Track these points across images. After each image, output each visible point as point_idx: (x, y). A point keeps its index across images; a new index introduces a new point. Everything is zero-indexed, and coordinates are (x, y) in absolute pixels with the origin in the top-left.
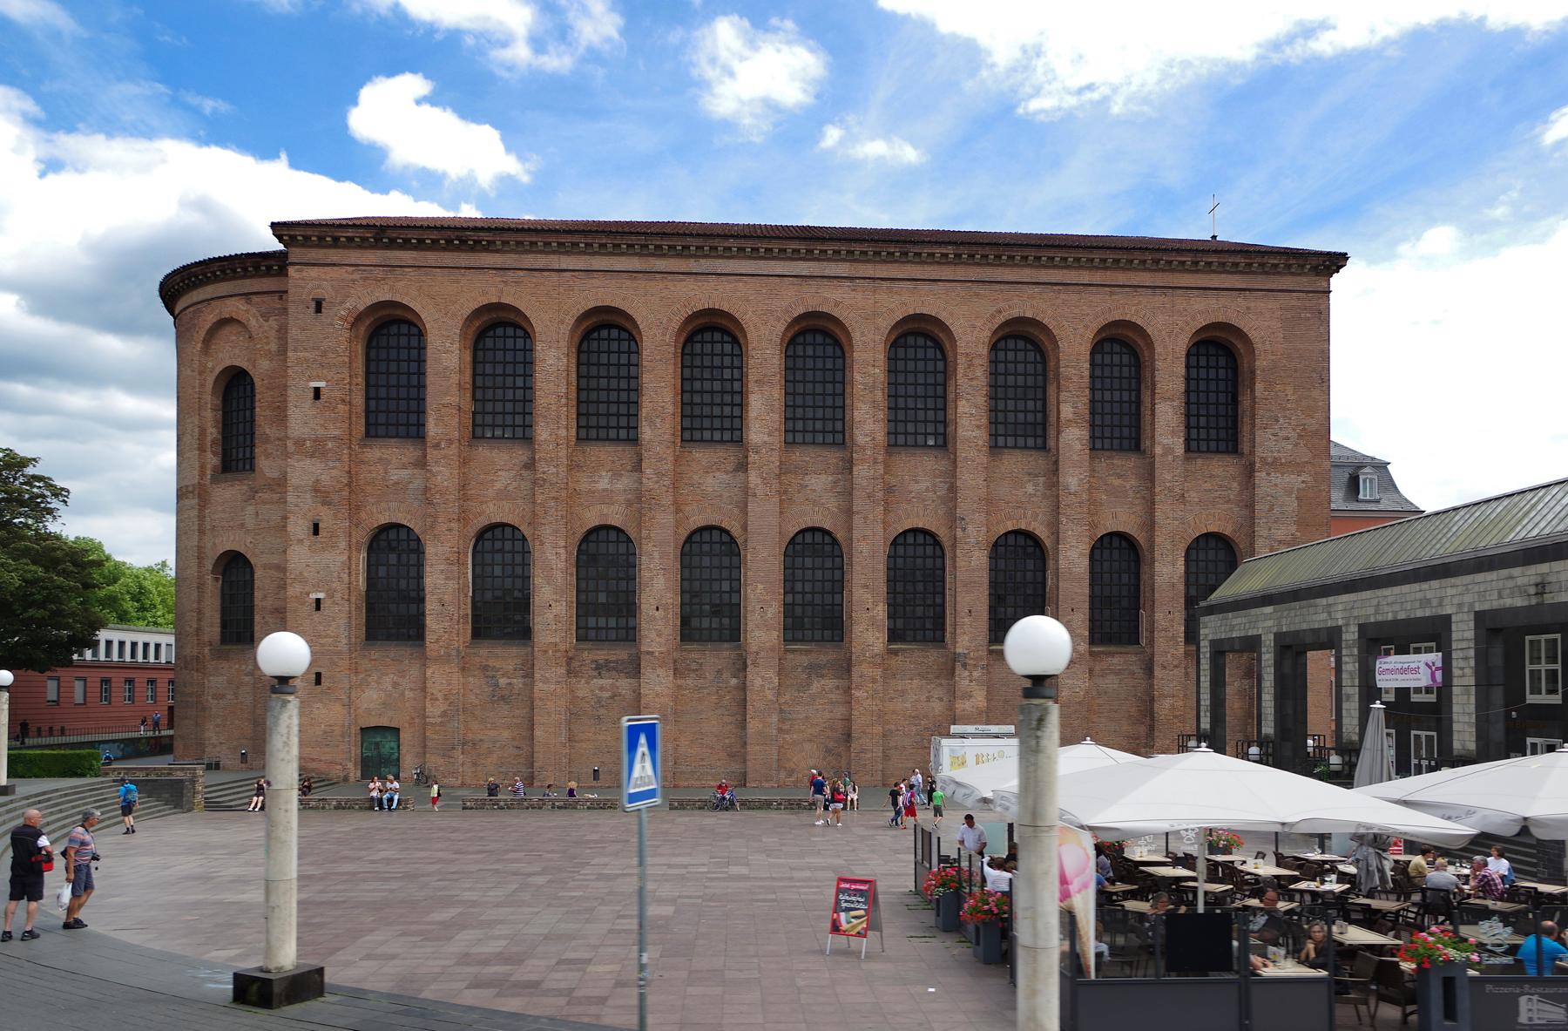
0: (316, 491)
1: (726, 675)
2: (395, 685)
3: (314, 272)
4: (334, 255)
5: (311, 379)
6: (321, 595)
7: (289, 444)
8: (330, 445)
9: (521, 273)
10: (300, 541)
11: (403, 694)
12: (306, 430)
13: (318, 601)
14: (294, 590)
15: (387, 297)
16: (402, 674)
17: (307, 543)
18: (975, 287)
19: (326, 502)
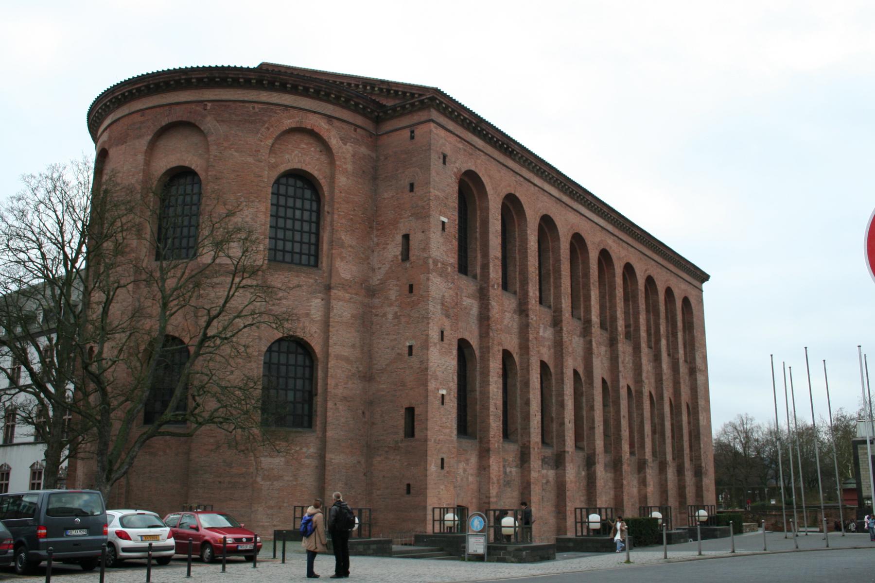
0: (443, 304)
1: (581, 469)
2: (465, 470)
3: (442, 133)
4: (451, 125)
5: (441, 213)
6: (444, 392)
7: (431, 261)
8: (449, 269)
9: (522, 179)
10: (435, 344)
11: (467, 479)
12: (439, 254)
13: (443, 395)
14: (432, 385)
15: (473, 168)
16: (467, 461)
17: (438, 346)
18: (641, 256)
19: (448, 316)
